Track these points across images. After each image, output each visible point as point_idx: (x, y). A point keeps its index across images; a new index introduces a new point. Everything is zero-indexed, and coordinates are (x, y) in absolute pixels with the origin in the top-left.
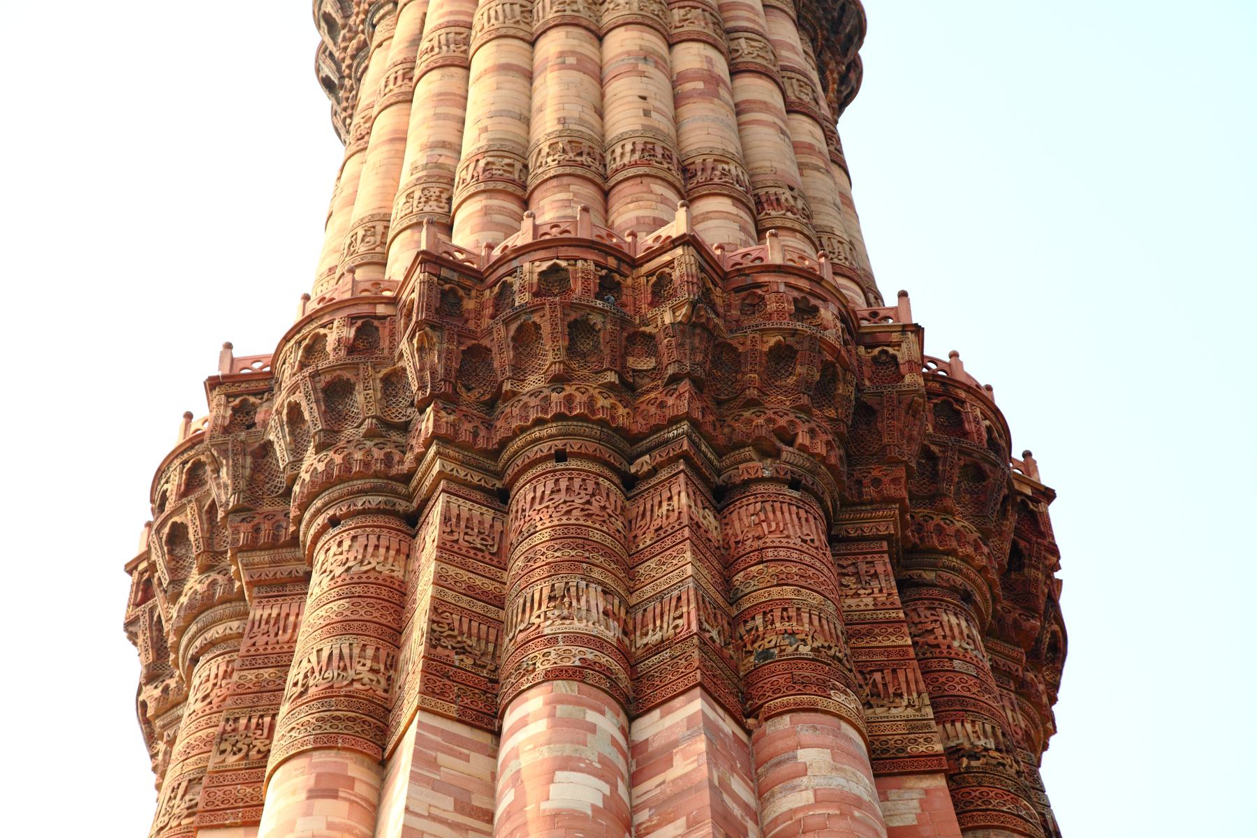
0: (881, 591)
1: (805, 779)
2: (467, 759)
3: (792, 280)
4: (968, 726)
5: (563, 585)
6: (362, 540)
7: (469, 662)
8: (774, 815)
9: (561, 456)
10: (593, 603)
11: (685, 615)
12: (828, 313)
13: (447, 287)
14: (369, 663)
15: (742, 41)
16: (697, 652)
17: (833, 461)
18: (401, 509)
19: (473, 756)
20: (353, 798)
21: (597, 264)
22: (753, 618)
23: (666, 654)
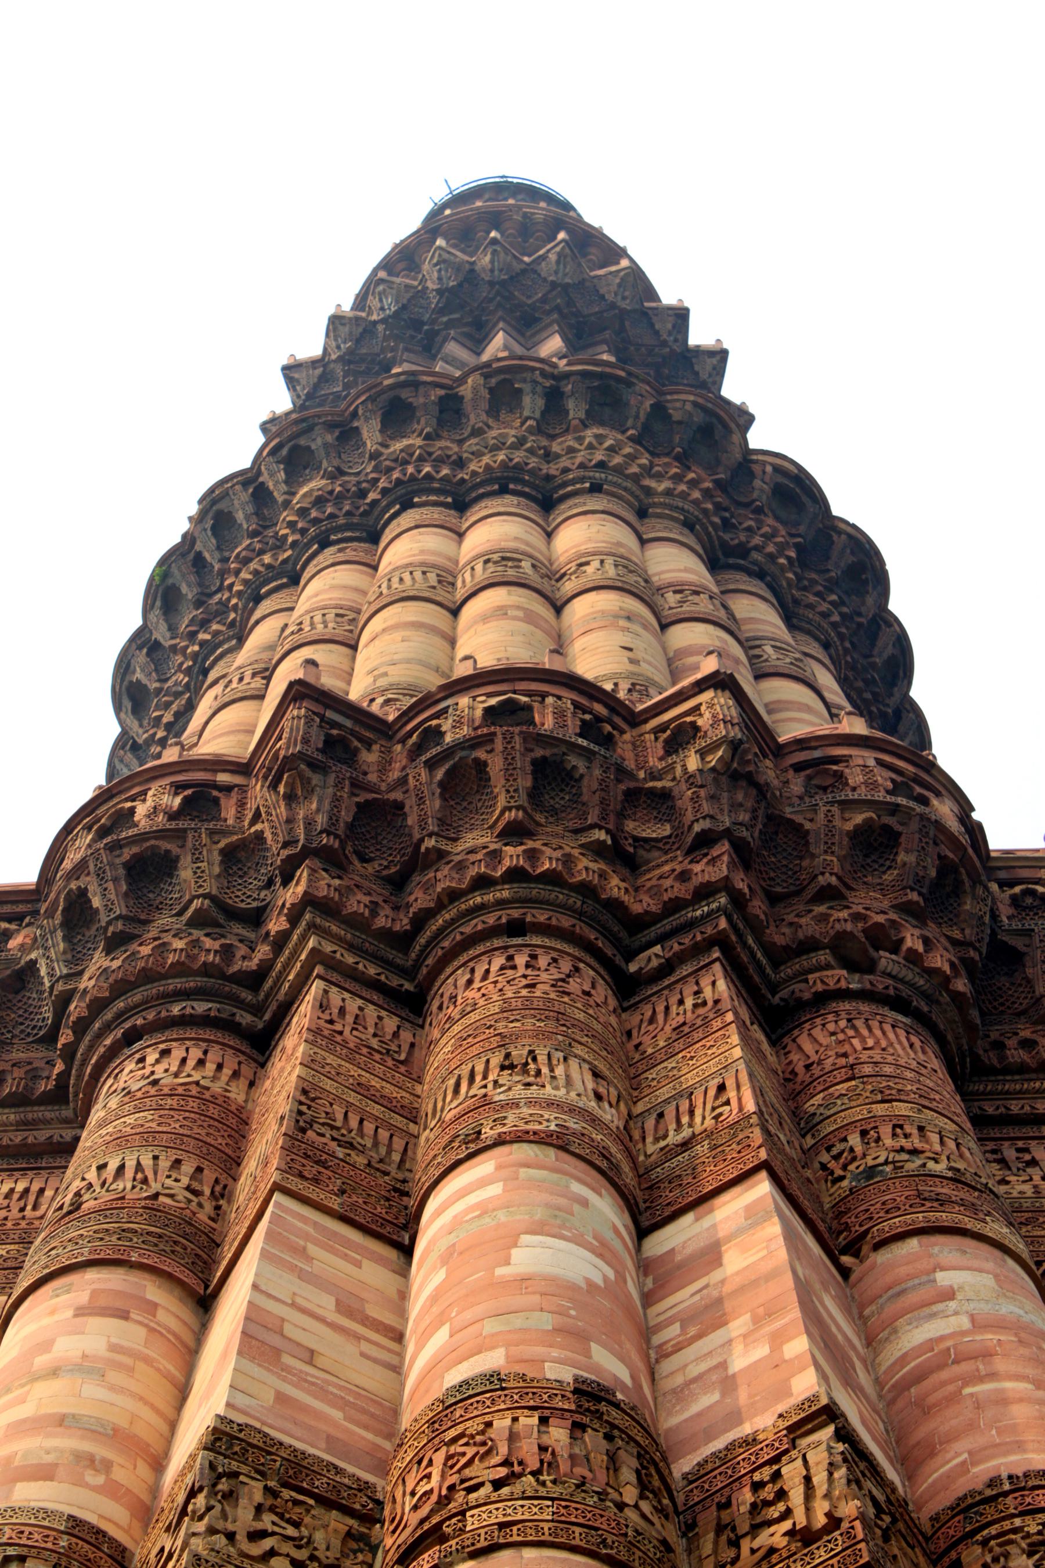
1: (952, 1305)
2: (358, 1265)
3: (888, 758)
5: (525, 1052)
6: (178, 1053)
7: (361, 1160)
8: (899, 1354)
9: (516, 928)
10: (575, 1074)
11: (734, 1103)
13: (335, 732)
14: (185, 1181)
15: (769, 649)
17: (961, 985)
18: (244, 1022)
20: (152, 1324)
21: (576, 705)
22: (845, 1140)
23: (702, 1149)
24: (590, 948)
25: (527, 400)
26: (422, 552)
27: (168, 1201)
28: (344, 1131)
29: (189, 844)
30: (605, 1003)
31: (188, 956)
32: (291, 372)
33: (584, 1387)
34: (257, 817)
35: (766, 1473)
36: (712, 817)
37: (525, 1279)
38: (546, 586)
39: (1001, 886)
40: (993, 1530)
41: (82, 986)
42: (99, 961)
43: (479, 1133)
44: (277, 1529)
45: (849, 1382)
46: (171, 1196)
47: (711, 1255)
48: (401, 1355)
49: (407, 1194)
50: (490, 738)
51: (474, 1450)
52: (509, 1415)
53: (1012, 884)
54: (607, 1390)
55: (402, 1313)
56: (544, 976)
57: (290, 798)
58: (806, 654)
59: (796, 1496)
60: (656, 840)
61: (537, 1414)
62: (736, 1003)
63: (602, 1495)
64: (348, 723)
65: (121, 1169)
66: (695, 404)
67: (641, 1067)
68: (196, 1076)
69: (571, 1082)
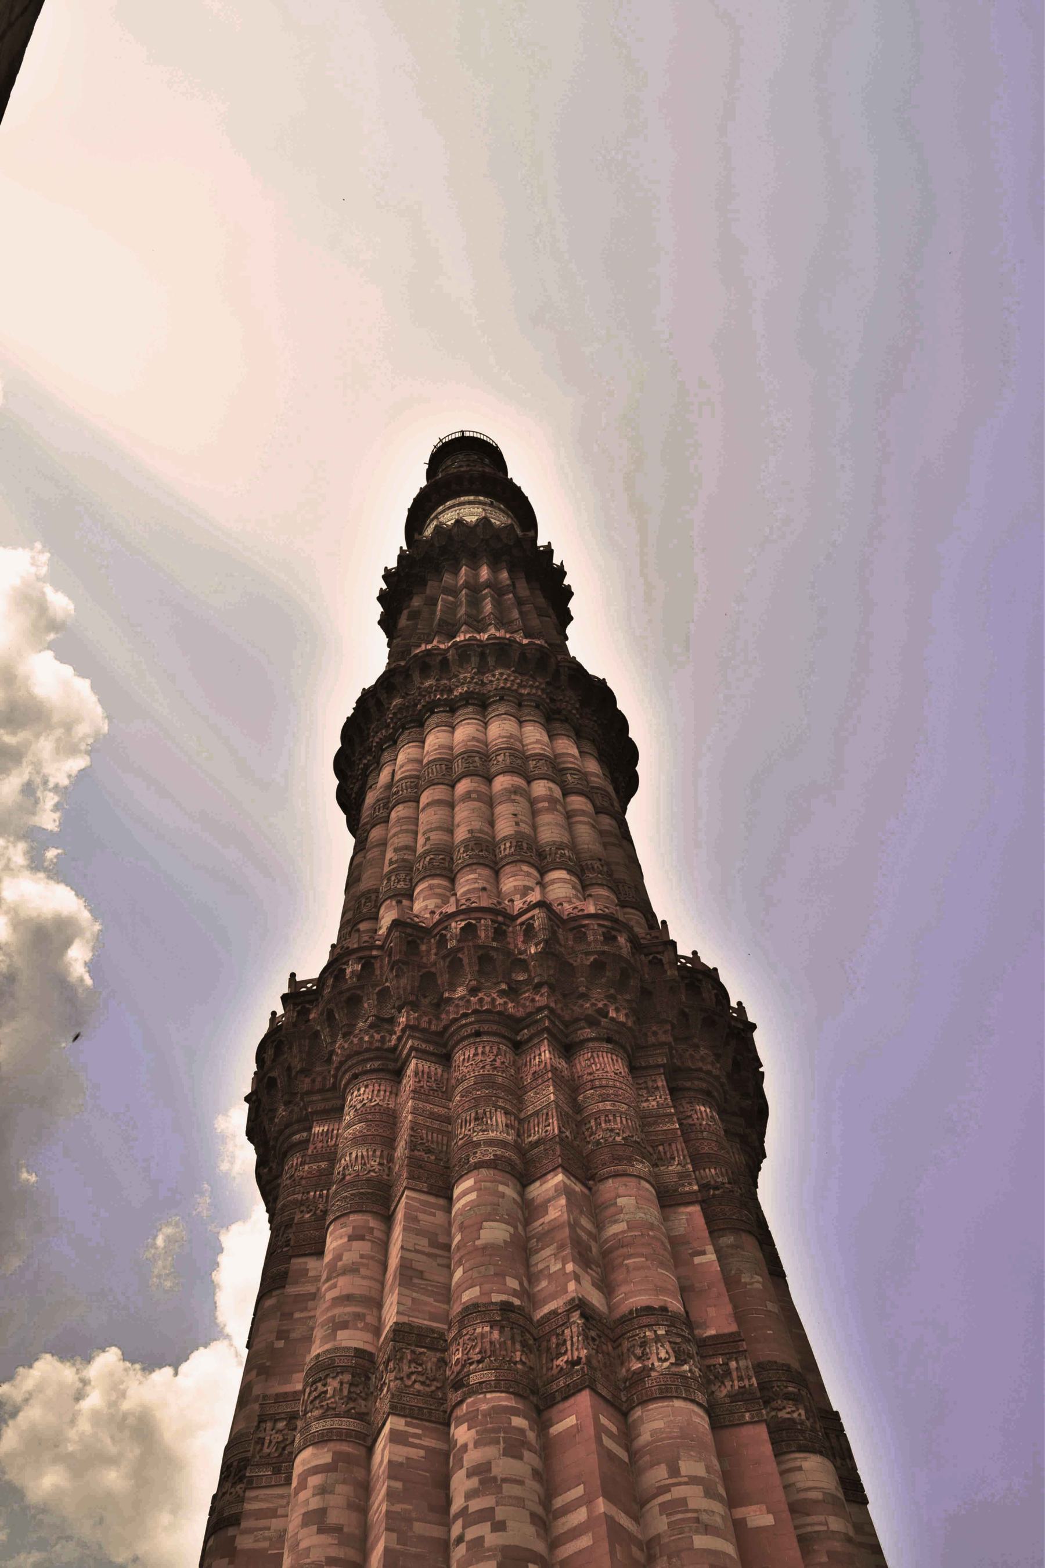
2: (434, 1215)
4: (713, 1170)
6: (371, 1087)
7: (433, 1158)
9: (478, 1034)
10: (499, 1120)
12: (622, 940)
14: (378, 1160)
17: (630, 1024)
23: (542, 1148)
24: (504, 1037)
25: (473, 659)
27: (372, 1174)
35: (559, 1331)
46: (373, 1171)
47: (544, 1207)
59: (569, 1343)
63: (510, 1361)
69: (498, 1126)
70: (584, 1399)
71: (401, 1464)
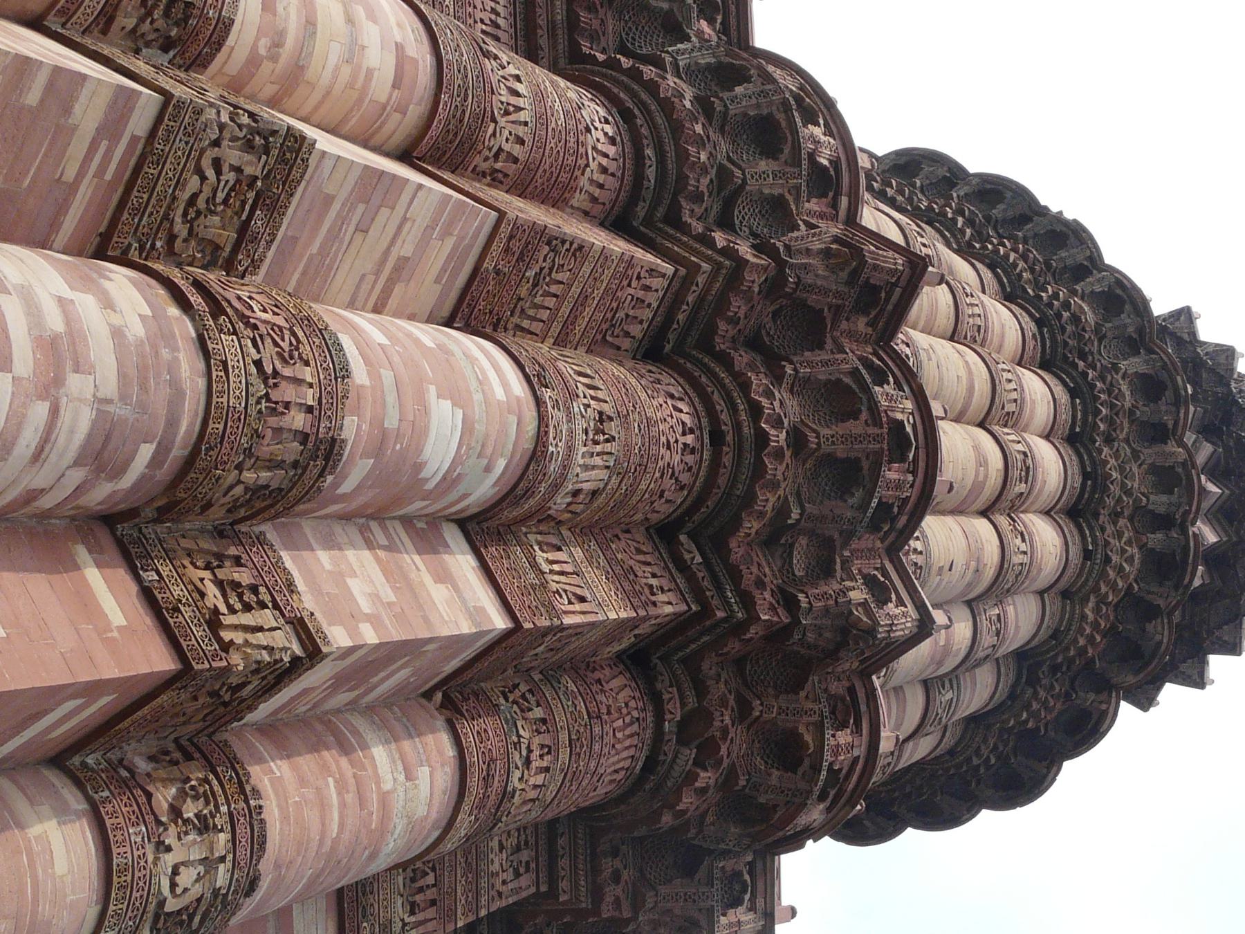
0: (504, 882)
1: (402, 778)
2: (437, 280)
5: (613, 433)
6: (612, 150)
7: (523, 291)
9: (717, 438)
10: (593, 474)
11: (571, 608)
13: (883, 295)
14: (506, 147)
15: (949, 695)
16: (547, 623)
17: (667, 819)
18: (638, 209)
19: (439, 287)
22: (538, 705)
23: (532, 578)
25: (1164, 498)
26: (1033, 402)
27: (490, 131)
28: (548, 279)
29: (788, 169)
30: (654, 511)
31: (694, 163)
32: (1185, 316)
33: (337, 448)
34: (810, 226)
35: (266, 598)
36: (810, 609)
37: (426, 411)
38: (1005, 504)
39: (749, 863)
40: (217, 788)
41: (669, 76)
42: (689, 93)
43: (546, 387)
44: (222, 183)
45: (339, 682)
46: (494, 134)
47: (443, 576)
48: (363, 309)
49: (495, 330)
50: (877, 422)
51: (287, 349)
52: (315, 381)
53: (750, 873)
54: (334, 467)
55: (397, 314)
56: (677, 458)
57: (826, 253)
58: (946, 727)
60: (791, 563)
61: (315, 404)
62: (653, 622)
63: (248, 452)
64: (890, 307)
65: (516, 93)
66: (1161, 642)
67: (600, 538)
68: (593, 165)
69: (588, 469)
70: (161, 661)
71: (67, 111)
